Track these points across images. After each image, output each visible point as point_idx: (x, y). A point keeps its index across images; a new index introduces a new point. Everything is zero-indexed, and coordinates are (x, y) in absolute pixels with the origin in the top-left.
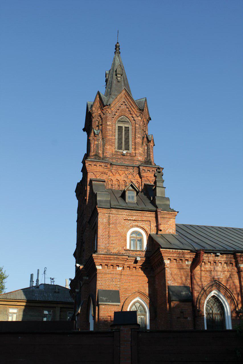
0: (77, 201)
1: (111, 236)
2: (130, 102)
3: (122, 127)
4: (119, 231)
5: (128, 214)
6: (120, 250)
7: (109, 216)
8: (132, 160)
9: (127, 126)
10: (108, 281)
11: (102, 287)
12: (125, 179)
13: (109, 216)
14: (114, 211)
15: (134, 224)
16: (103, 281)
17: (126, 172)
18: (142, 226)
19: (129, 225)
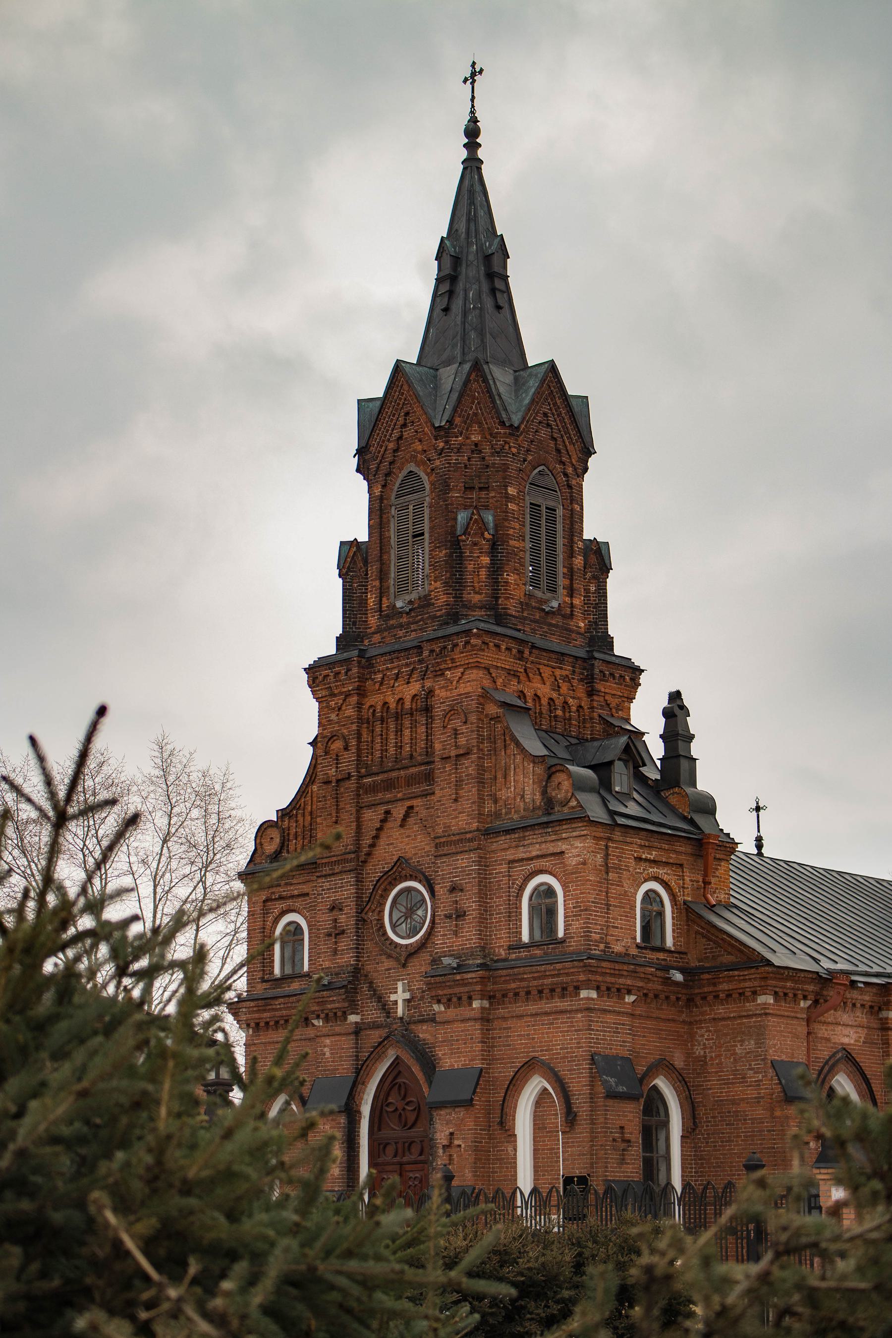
0: (313, 706)
1: (610, 905)
2: (562, 421)
3: (539, 506)
4: (626, 892)
5: (643, 843)
6: (629, 947)
7: (607, 847)
8: (567, 629)
9: (551, 504)
10: (609, 1032)
11: (598, 1048)
12: (555, 695)
13: (607, 847)
14: (617, 835)
15: (651, 870)
16: (601, 1031)
17: (558, 672)
18: (666, 878)
19: (641, 873)
